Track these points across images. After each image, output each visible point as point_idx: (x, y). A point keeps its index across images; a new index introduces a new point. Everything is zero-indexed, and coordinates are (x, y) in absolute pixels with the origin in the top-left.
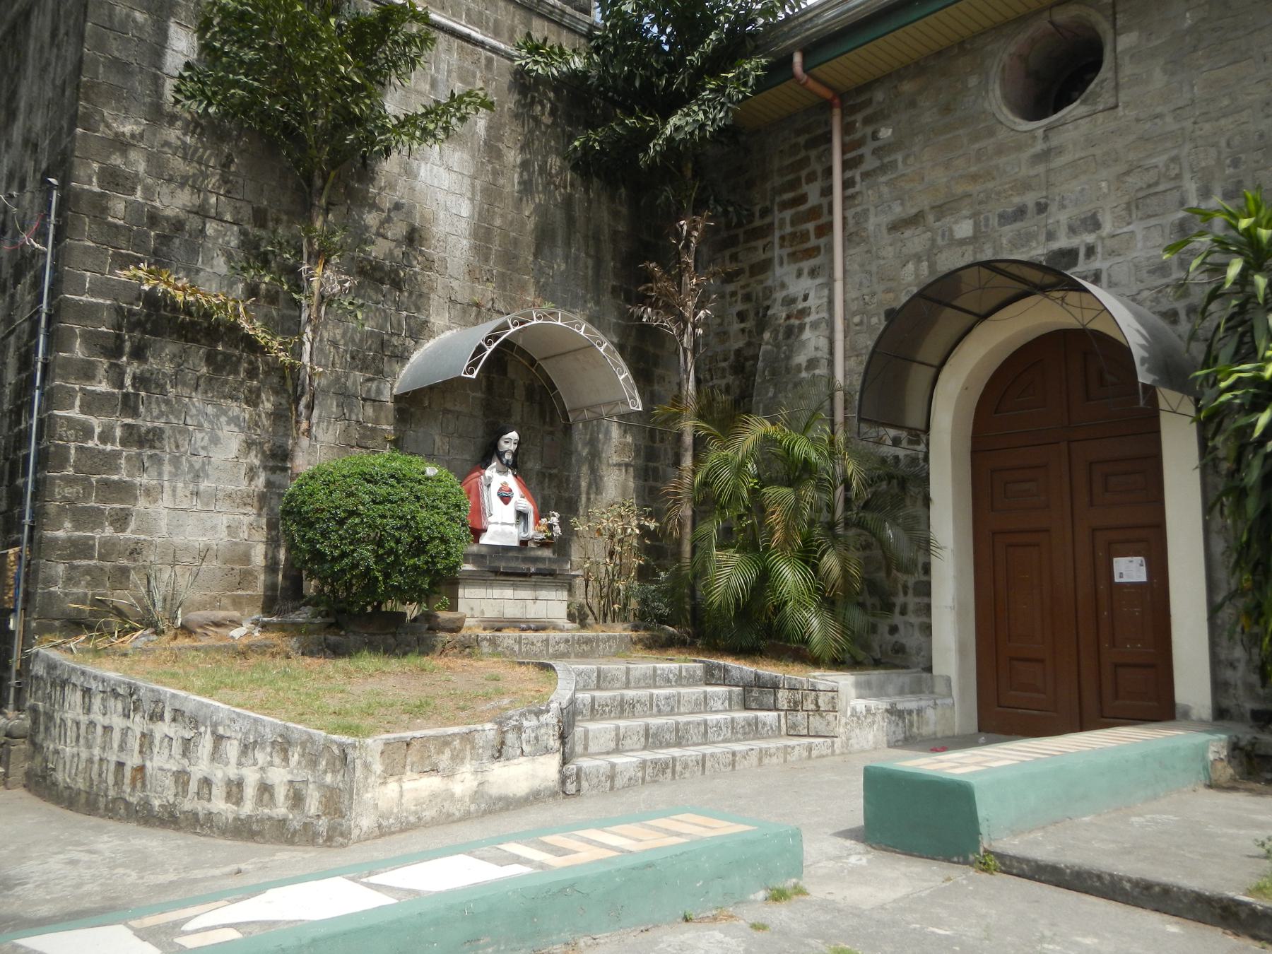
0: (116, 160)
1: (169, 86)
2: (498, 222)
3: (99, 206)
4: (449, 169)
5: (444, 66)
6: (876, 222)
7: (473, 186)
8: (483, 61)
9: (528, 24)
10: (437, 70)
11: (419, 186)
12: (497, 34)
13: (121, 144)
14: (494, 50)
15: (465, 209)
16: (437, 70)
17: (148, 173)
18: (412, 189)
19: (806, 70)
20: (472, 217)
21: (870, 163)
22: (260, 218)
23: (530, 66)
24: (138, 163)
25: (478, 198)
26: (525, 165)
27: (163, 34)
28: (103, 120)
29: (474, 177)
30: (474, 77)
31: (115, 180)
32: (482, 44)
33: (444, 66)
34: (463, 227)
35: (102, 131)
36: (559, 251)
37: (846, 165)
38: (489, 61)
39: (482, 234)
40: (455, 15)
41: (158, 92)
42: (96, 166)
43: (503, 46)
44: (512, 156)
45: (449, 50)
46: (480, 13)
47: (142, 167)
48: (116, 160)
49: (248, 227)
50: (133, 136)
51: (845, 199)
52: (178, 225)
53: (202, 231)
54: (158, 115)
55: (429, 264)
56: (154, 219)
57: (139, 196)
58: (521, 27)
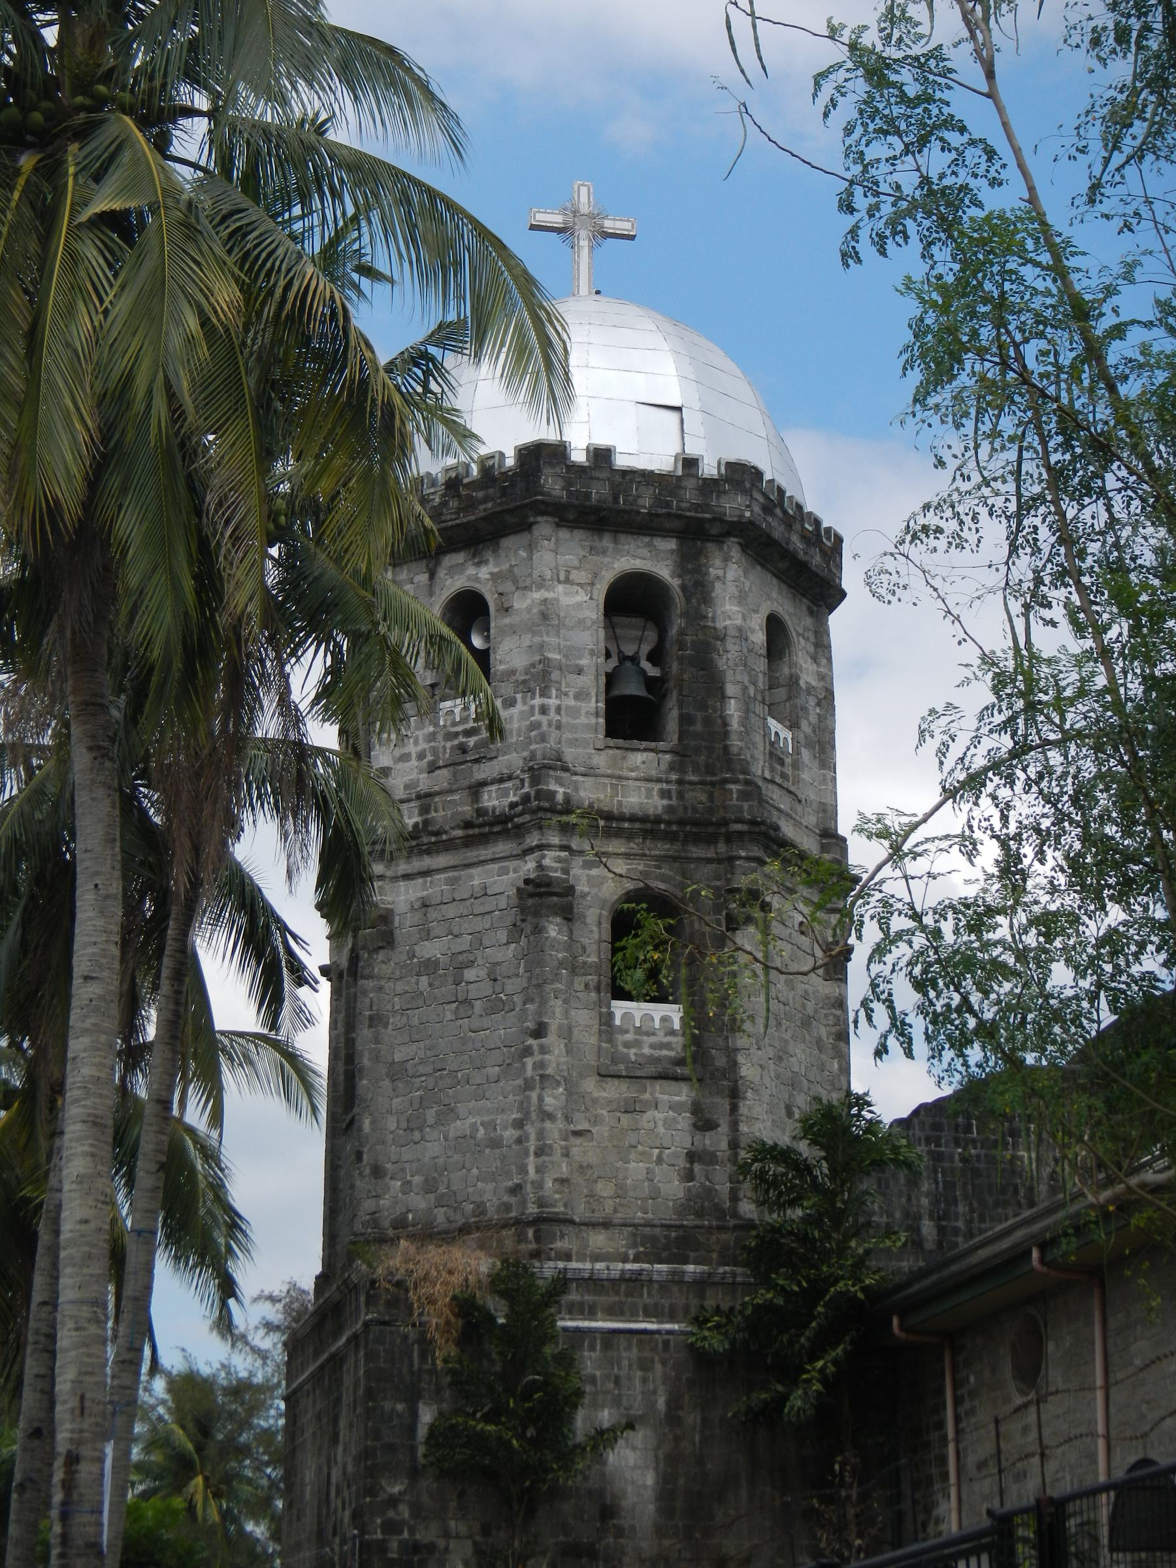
0: (391, 1514)
1: (421, 1450)
2: (682, 1481)
3: (382, 1547)
4: (634, 1448)
5: (625, 1363)
6: (971, 1460)
7: (656, 1456)
8: (660, 1346)
9: (702, 1296)
10: (620, 1368)
11: (609, 1469)
12: (672, 1318)
13: (393, 1502)
14: (669, 1332)
15: (650, 1479)
16: (620, 1368)
17: (411, 1515)
18: (603, 1475)
19: (901, 1328)
20: (657, 1483)
21: (967, 1405)
22: (486, 1531)
23: (699, 1344)
24: (405, 1512)
25: (662, 1465)
26: (705, 1420)
27: (414, 1415)
28: (381, 1487)
29: (657, 1448)
30: (652, 1361)
31: (391, 1527)
32: (658, 1332)
33: (625, 1363)
34: (649, 1494)
35: (382, 1496)
36: (744, 1493)
37: (957, 1401)
38: (666, 1343)
39: (666, 1495)
40: (633, 1317)
41: (414, 1458)
42: (379, 1521)
43: (676, 1327)
44: (692, 1418)
45: (628, 1348)
46: (656, 1305)
47: (406, 1515)
48: (391, 1514)
49: (478, 1538)
50: (400, 1493)
51: (958, 1432)
52: (431, 1548)
53: (447, 1549)
54: (414, 1473)
55: (620, 1532)
56: (416, 1548)
57: (406, 1535)
58: (694, 1302)
